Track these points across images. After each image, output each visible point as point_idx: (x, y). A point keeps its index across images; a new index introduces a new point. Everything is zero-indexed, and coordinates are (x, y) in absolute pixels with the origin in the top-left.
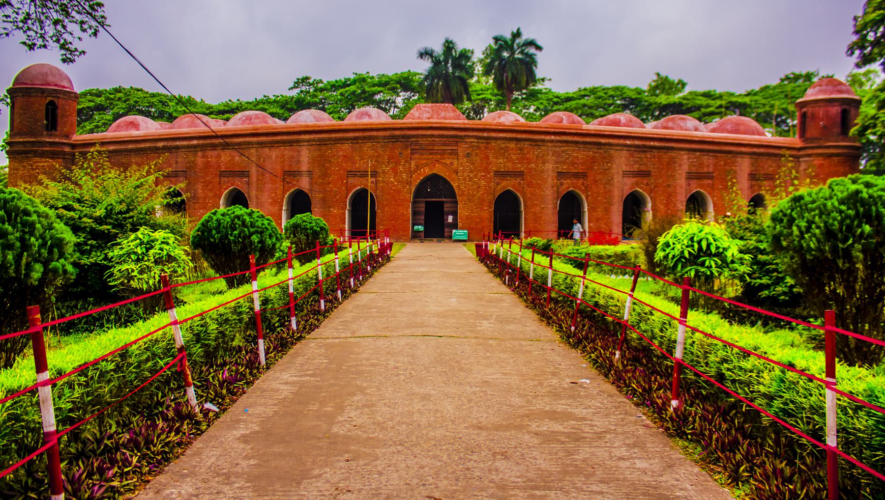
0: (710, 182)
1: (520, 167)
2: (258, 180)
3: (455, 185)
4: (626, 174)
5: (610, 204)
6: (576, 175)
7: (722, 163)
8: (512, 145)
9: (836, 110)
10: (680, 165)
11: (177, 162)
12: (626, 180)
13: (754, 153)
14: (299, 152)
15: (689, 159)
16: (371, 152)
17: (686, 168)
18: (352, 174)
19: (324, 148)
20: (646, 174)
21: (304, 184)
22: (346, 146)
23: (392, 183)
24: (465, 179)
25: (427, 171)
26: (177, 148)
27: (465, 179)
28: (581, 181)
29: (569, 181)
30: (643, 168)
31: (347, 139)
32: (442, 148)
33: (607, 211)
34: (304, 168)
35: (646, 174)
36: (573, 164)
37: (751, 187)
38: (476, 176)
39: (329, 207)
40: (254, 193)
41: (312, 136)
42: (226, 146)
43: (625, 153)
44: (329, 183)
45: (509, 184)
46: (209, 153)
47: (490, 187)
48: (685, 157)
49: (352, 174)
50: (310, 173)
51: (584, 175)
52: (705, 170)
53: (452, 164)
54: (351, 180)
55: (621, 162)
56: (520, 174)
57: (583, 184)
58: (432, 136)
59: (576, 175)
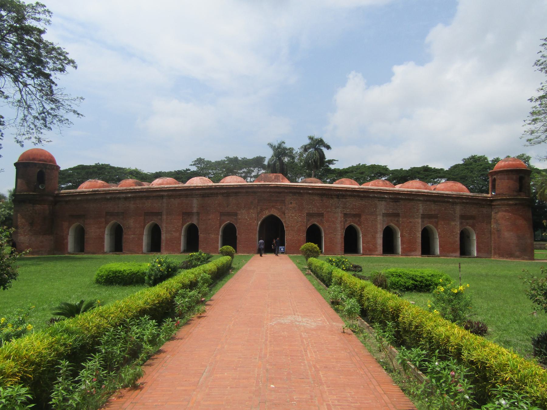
0: (436, 220)
3: (283, 221)
5: (376, 232)
6: (355, 216)
7: (443, 209)
8: (316, 198)
10: (418, 210)
13: (463, 203)
18: (222, 214)
20: (397, 215)
22: (220, 197)
23: (247, 219)
24: (289, 218)
25: (267, 213)
27: (289, 218)
28: (358, 219)
29: (351, 219)
33: (374, 238)
35: (397, 215)
38: (296, 216)
39: (209, 234)
40: (164, 225)
42: (148, 198)
43: (383, 203)
44: (209, 219)
45: (315, 221)
47: (304, 222)
52: (433, 213)
53: (282, 208)
58: (270, 192)
59: (355, 216)
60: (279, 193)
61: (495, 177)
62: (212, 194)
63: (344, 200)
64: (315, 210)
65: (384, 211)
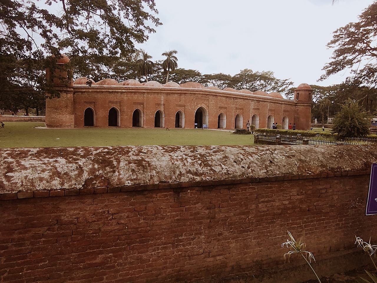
1: (226, 106)
2: (147, 106)
4: (254, 109)
6: (240, 109)
8: (224, 98)
9: (307, 93)
10: (267, 107)
11: (117, 98)
12: (253, 111)
14: (161, 97)
15: (269, 105)
16: (184, 99)
17: (268, 107)
18: (177, 106)
19: (169, 96)
20: (258, 109)
21: (162, 109)
22: (176, 95)
25: (199, 106)
26: (118, 92)
27: (210, 109)
30: (258, 107)
31: (177, 93)
32: (204, 98)
34: (162, 103)
35: (258, 109)
36: (240, 105)
37: (283, 114)
41: (165, 92)
42: (135, 93)
45: (222, 111)
46: (129, 95)
47: (218, 112)
48: (268, 105)
49: (177, 106)
50: (164, 105)
51: (242, 109)
54: (178, 108)
55: (252, 105)
56: (226, 108)
57: (242, 112)
58: (202, 94)
59: (240, 109)
60: (207, 95)
61: (299, 92)
62: (172, 93)
63: (236, 100)
64: (223, 105)
65: (253, 107)
